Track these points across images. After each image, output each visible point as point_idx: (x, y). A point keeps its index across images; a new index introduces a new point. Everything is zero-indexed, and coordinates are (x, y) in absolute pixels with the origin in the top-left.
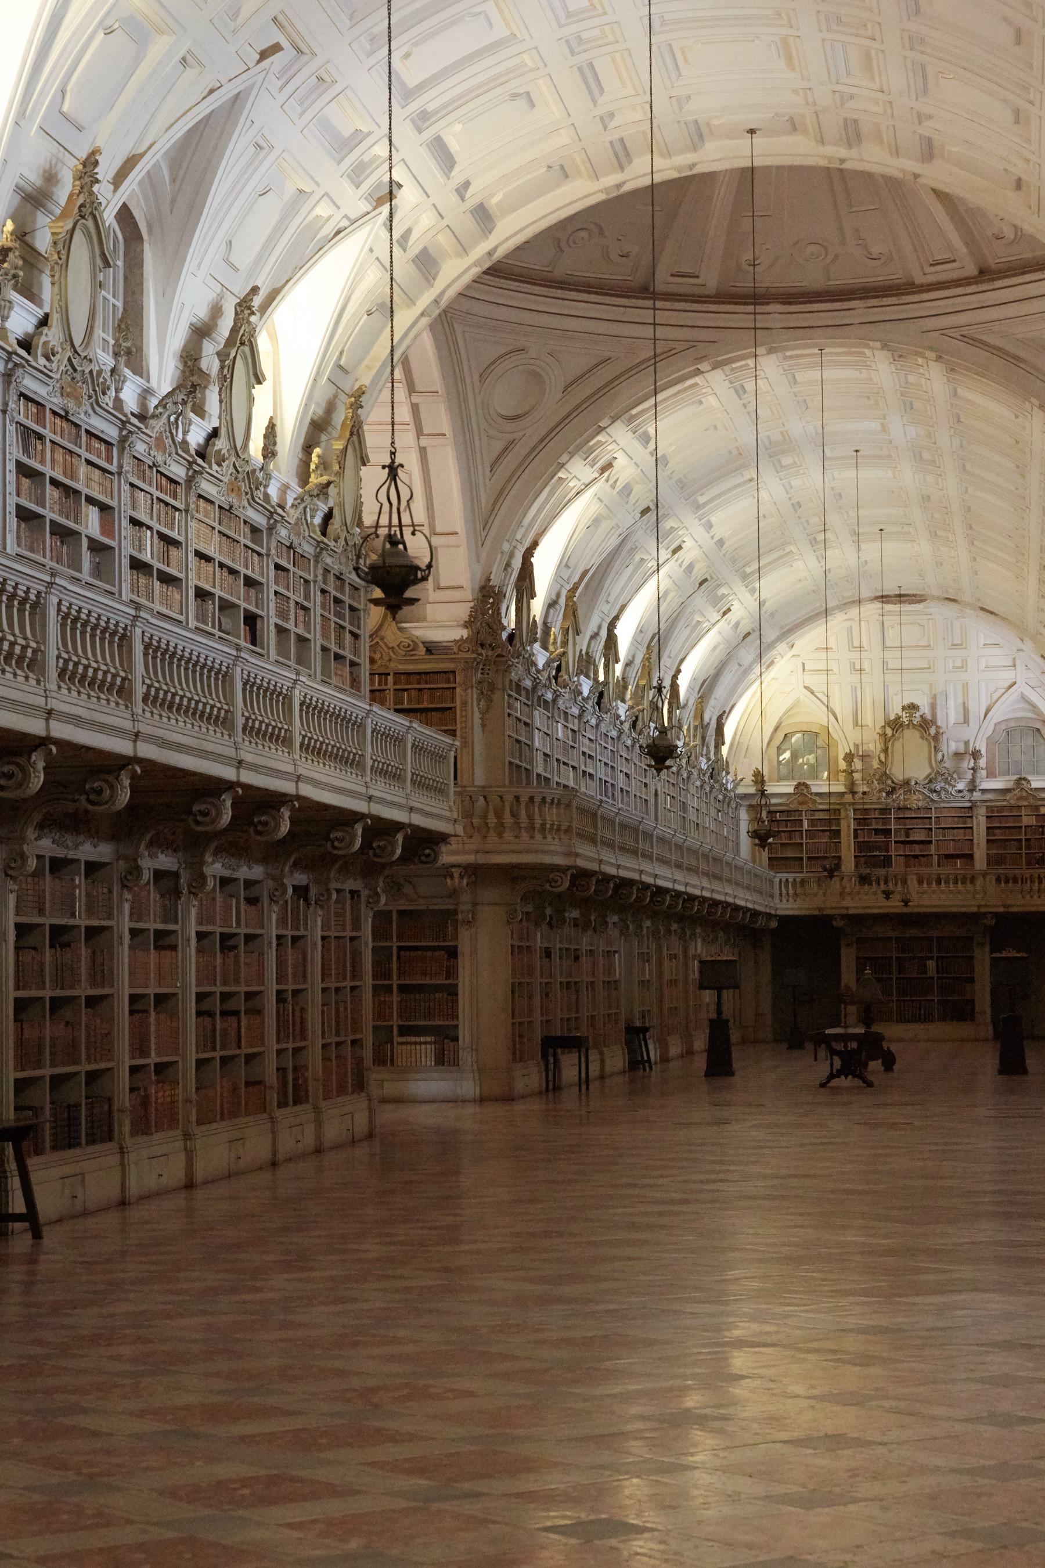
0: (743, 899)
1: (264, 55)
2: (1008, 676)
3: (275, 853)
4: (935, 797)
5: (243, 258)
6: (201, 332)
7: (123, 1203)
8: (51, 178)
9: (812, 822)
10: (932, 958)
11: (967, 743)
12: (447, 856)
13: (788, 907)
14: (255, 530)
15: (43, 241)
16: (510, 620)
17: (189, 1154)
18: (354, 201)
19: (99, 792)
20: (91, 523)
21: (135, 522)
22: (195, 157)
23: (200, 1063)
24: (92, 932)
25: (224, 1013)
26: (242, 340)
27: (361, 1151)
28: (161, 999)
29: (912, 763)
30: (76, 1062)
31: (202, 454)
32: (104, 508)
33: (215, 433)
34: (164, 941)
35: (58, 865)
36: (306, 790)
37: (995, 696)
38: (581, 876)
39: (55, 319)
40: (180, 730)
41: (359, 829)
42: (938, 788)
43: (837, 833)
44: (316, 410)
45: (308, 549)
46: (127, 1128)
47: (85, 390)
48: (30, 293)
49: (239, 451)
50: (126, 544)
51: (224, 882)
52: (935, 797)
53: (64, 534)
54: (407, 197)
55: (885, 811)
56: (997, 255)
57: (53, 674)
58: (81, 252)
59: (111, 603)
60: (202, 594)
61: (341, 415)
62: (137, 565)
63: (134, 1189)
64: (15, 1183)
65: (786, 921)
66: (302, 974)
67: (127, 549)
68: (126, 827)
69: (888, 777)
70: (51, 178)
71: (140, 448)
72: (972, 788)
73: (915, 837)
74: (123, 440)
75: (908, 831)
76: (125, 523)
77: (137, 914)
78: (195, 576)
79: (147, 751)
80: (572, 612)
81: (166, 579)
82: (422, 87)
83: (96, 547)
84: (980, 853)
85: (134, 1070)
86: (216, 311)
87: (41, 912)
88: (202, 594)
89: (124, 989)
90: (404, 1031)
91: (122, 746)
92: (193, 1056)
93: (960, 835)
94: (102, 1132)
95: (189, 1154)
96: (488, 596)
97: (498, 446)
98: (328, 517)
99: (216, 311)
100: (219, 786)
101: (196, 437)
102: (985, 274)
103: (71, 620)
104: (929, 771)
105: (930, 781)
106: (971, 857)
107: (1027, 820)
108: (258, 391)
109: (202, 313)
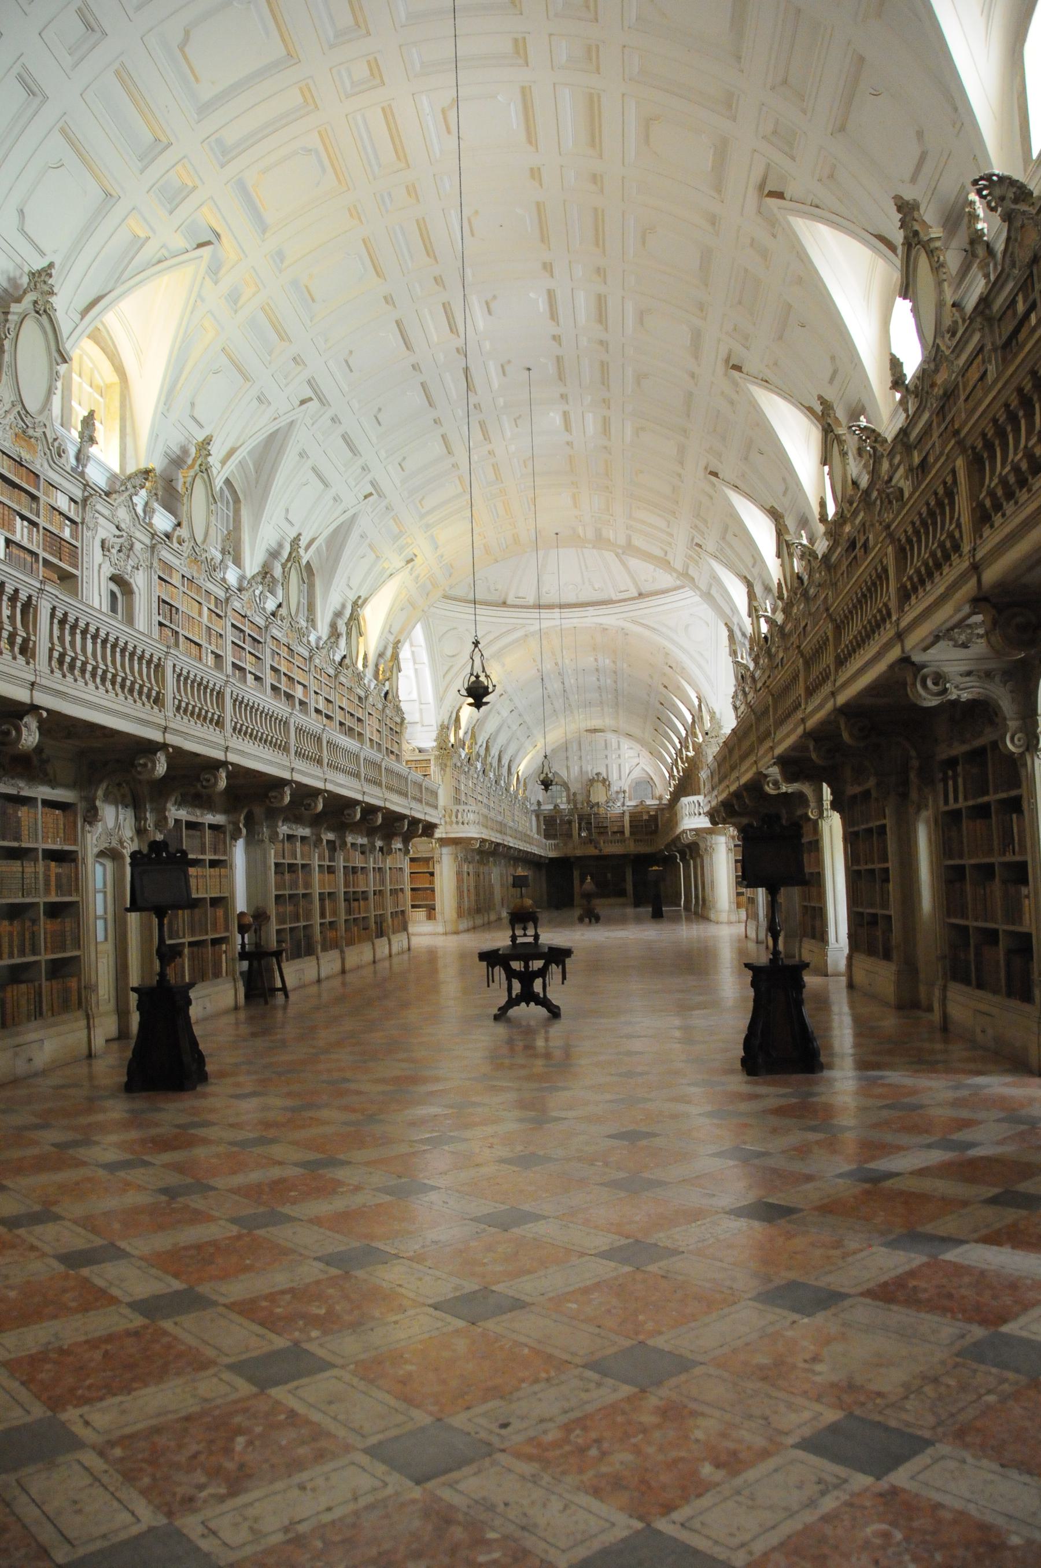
0: (536, 850)
1: (366, 497)
2: (636, 761)
3: (371, 832)
5: (354, 583)
6: (338, 614)
7: (319, 981)
8: (280, 545)
12: (439, 833)
13: (552, 854)
14: (360, 698)
15: (278, 572)
16: (452, 740)
17: (343, 960)
18: (397, 562)
19: (310, 805)
20: (299, 692)
21: (316, 693)
22: (338, 539)
23: (346, 921)
24: (303, 866)
25: (355, 900)
26: (354, 617)
27: (406, 956)
28: (329, 894)
29: (599, 796)
30: (298, 921)
31: (340, 664)
32: (305, 686)
33: (345, 657)
34: (331, 870)
35: (290, 837)
36: (388, 805)
38: (483, 841)
39: (284, 604)
40: (341, 778)
41: (406, 822)
44: (381, 648)
45: (380, 706)
46: (319, 950)
47: (296, 635)
48: (272, 592)
49: (354, 664)
50: (312, 702)
51: (353, 844)
53: (289, 697)
54: (418, 561)
55: (590, 815)
56: (646, 588)
57: (293, 752)
58: (294, 577)
59: (313, 723)
60: (341, 724)
61: (389, 653)
62: (317, 711)
63: (323, 975)
64: (277, 974)
65: (551, 859)
66: (383, 882)
67: (313, 705)
68: (316, 821)
70: (280, 545)
71: (317, 661)
72: (623, 805)
74: (311, 657)
76: (312, 693)
77: (321, 858)
78: (339, 716)
79: (330, 787)
80: (473, 736)
81: (328, 717)
82: (428, 513)
83: (302, 703)
85: (321, 924)
86: (344, 606)
87: (284, 858)
88: (341, 724)
89: (316, 890)
90: (413, 906)
91: (319, 785)
92: (343, 917)
94: (310, 951)
95: (343, 960)
96: (444, 729)
97: (446, 668)
98: (387, 694)
99: (344, 606)
100: (357, 802)
101: (338, 658)
102: (641, 595)
103: (299, 730)
106: (623, 833)
107: (645, 817)
108: (361, 639)
109: (339, 607)
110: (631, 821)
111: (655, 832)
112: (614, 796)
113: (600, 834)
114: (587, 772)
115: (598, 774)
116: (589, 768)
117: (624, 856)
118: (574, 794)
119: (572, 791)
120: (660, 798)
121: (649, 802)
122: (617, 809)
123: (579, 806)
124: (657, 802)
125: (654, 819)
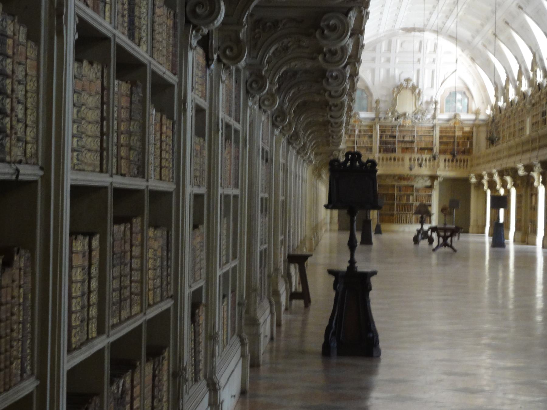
4: (417, 121)
9: (360, 131)
10: (413, 195)
11: (432, 98)
29: (406, 105)
37: (446, 77)
42: (419, 117)
43: (371, 137)
52: (417, 121)
69: (397, 111)
72: (434, 117)
73: (407, 139)
75: (404, 137)
84: (437, 148)
93: (427, 139)
104: (414, 109)
105: (415, 114)
106: (431, 150)
107: (458, 133)
110: (441, 137)
111: (468, 152)
112: (424, 106)
113: (405, 150)
114: (394, 77)
115: (407, 80)
116: (397, 72)
117: (433, 178)
118: (377, 102)
119: (375, 96)
120: (477, 113)
121: (463, 116)
122: (427, 121)
123: (382, 115)
124: (473, 117)
125: (468, 137)
